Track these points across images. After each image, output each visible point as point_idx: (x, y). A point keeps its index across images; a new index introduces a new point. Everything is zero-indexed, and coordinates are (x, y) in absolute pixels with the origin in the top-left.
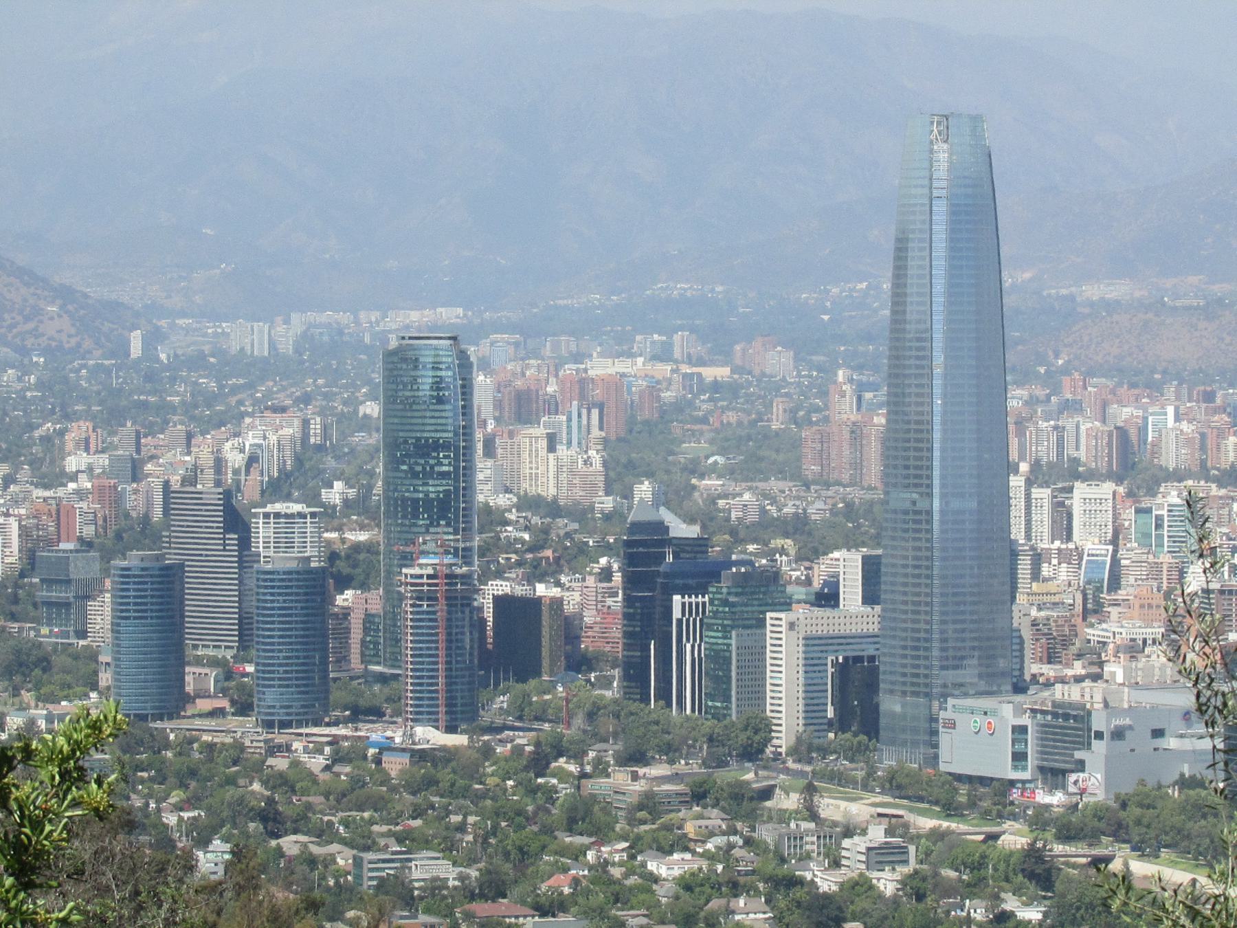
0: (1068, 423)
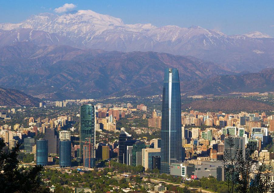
0: (191, 118)
